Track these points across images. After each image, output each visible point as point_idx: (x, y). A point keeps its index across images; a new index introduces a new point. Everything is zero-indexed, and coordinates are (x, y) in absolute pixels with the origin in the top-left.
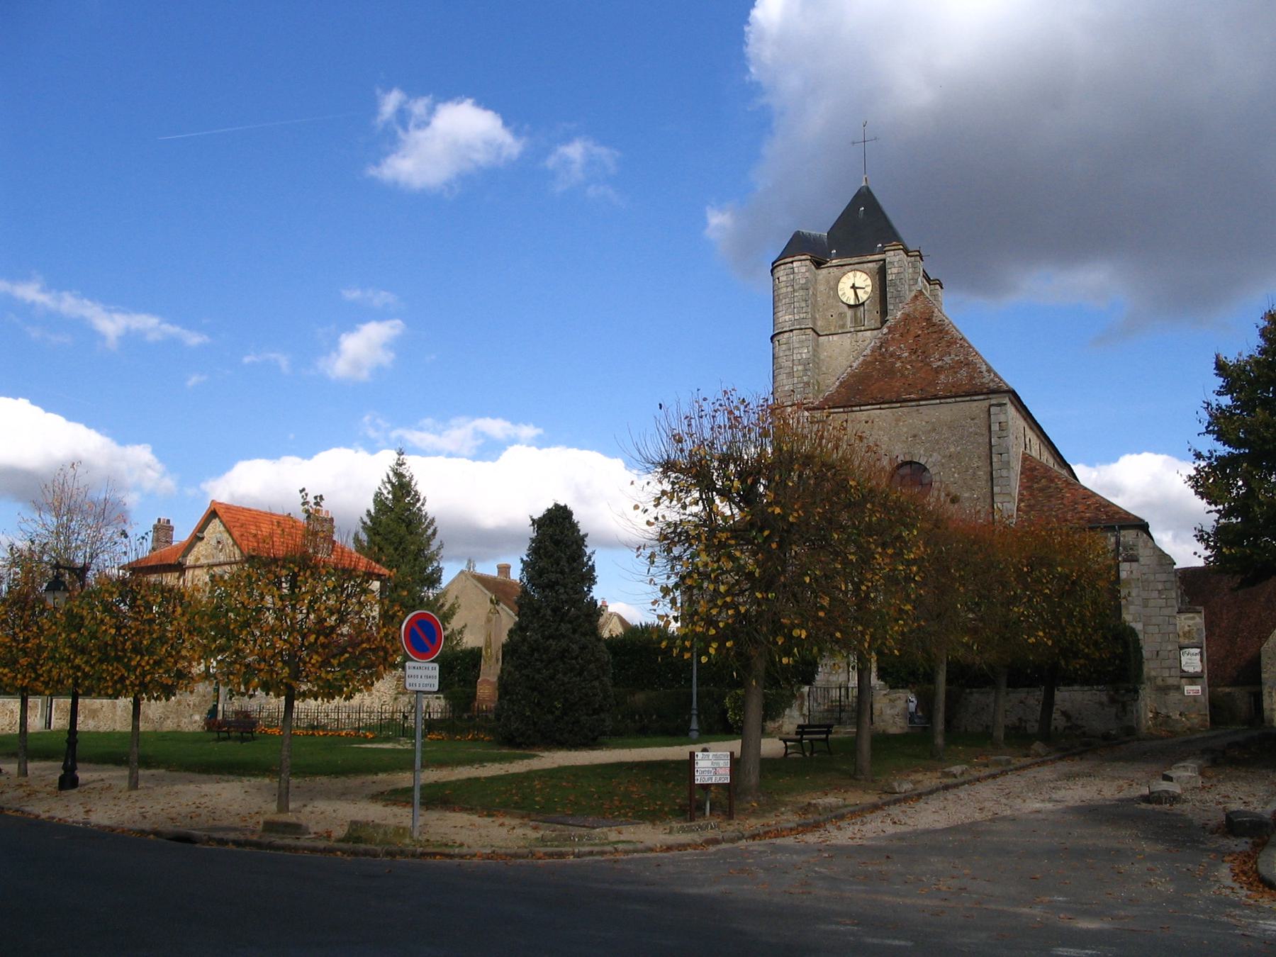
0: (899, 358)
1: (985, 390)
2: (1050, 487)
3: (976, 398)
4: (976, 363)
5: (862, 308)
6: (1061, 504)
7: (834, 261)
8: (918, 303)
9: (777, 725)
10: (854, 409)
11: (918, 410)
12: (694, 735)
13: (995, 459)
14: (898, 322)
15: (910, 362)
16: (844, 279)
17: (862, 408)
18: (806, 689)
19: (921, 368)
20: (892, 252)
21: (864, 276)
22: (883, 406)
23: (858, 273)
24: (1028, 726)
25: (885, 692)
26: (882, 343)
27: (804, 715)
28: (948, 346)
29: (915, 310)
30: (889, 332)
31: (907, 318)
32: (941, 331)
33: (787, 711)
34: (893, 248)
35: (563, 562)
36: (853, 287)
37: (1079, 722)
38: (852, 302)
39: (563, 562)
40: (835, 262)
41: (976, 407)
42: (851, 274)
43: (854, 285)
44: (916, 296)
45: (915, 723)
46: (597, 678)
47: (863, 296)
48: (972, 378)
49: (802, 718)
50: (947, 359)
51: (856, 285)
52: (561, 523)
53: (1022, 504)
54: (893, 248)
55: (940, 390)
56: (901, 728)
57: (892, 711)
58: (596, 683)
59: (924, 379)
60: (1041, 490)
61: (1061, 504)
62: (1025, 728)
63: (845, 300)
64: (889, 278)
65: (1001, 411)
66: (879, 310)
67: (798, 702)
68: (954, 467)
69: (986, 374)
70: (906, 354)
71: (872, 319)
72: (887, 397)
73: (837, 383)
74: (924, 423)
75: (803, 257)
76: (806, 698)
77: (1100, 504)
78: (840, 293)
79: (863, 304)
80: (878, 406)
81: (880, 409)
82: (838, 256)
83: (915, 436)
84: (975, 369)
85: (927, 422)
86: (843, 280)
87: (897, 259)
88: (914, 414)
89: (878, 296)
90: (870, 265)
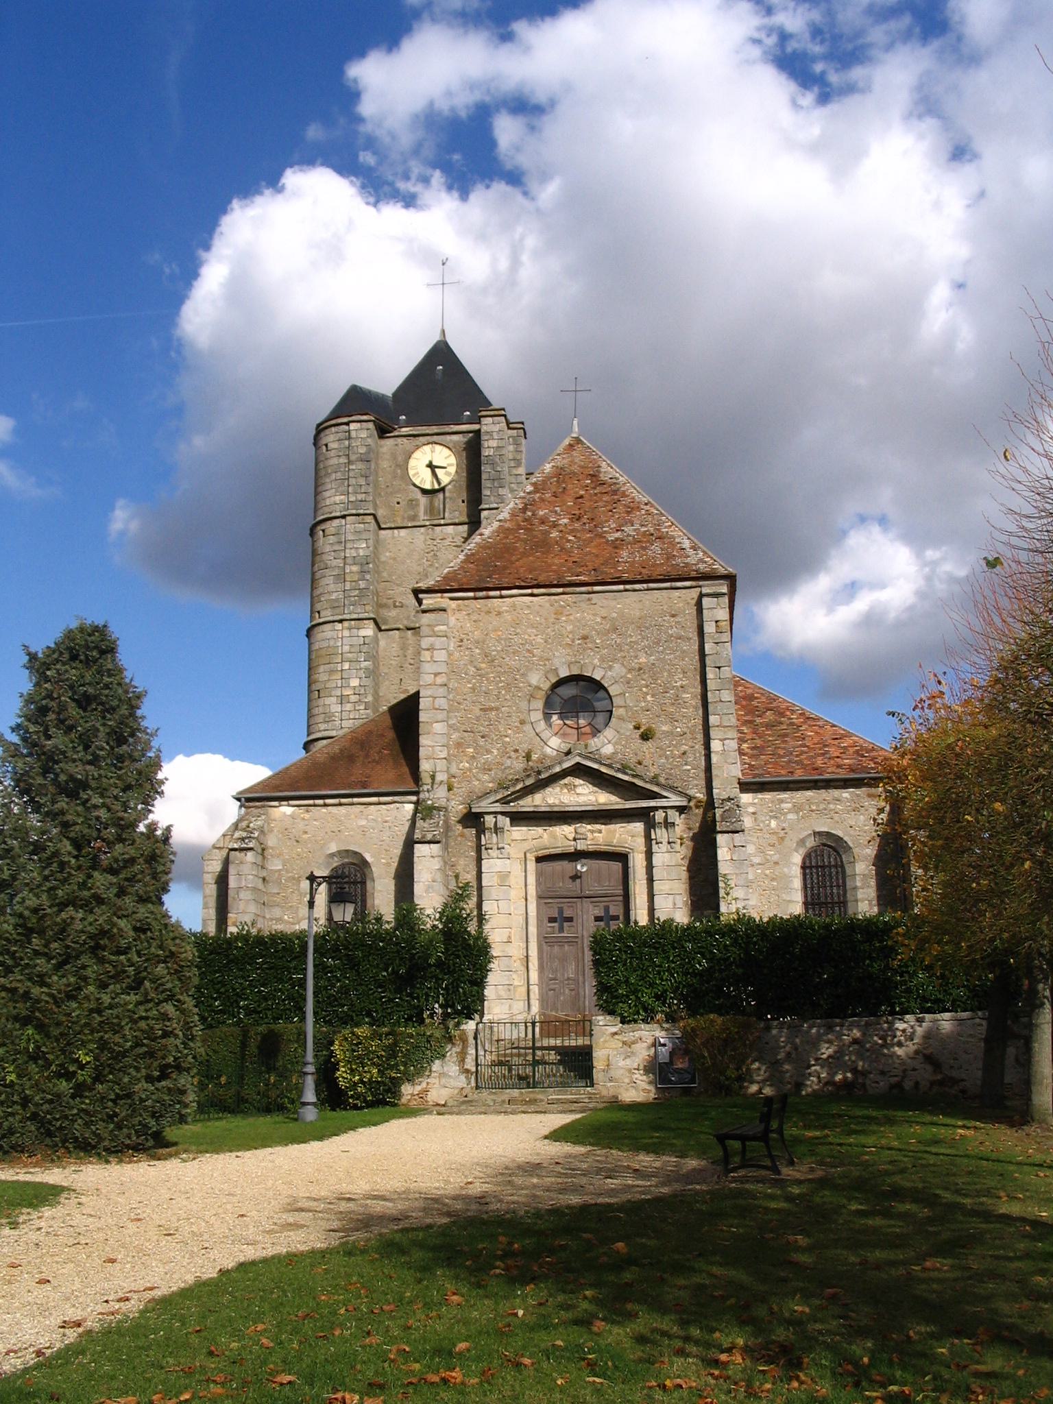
0: (555, 525)
1: (693, 574)
2: (781, 723)
3: (679, 584)
4: (673, 537)
5: (441, 495)
6: (801, 746)
7: (404, 429)
8: (574, 453)
9: (418, 1088)
10: (492, 593)
11: (589, 600)
12: (310, 1114)
13: (710, 675)
14: (548, 478)
15: (572, 531)
16: (417, 454)
17: (504, 592)
18: (470, 1026)
19: (591, 540)
20: (490, 419)
21: (447, 452)
22: (536, 591)
23: (438, 448)
24: (868, 1082)
25: (614, 1029)
26: (526, 505)
27: (467, 1071)
28: (628, 513)
29: (572, 463)
30: (536, 491)
31: (560, 473)
32: (615, 492)
33: (437, 1065)
34: (492, 413)
35: (101, 741)
36: (431, 466)
37: (955, 1074)
38: (428, 486)
39: (101, 741)
40: (405, 430)
41: (682, 598)
42: (427, 448)
43: (431, 462)
44: (571, 445)
45: (670, 1082)
46: (171, 998)
47: (445, 479)
48: (670, 557)
49: (463, 1077)
50: (628, 529)
51: (435, 463)
52: (95, 661)
53: (745, 746)
54: (492, 413)
55: (623, 572)
56: (644, 1090)
57: (628, 1061)
58: (169, 1008)
59: (597, 556)
60: (769, 726)
61: (801, 746)
62: (864, 1085)
63: (417, 483)
64: (485, 452)
65: (718, 604)
66: (465, 498)
67: (457, 1049)
68: (647, 686)
69: (691, 552)
70: (566, 521)
71: (457, 509)
72: (542, 578)
73: (462, 557)
74: (599, 620)
75: (365, 418)
76: (471, 1041)
77: (861, 746)
78: (411, 473)
79: (443, 490)
80: (529, 591)
81: (532, 595)
82: (408, 424)
83: (585, 638)
84: (673, 544)
85: (604, 618)
86: (415, 455)
87: (496, 428)
88: (583, 605)
89: (464, 479)
90: (455, 438)
